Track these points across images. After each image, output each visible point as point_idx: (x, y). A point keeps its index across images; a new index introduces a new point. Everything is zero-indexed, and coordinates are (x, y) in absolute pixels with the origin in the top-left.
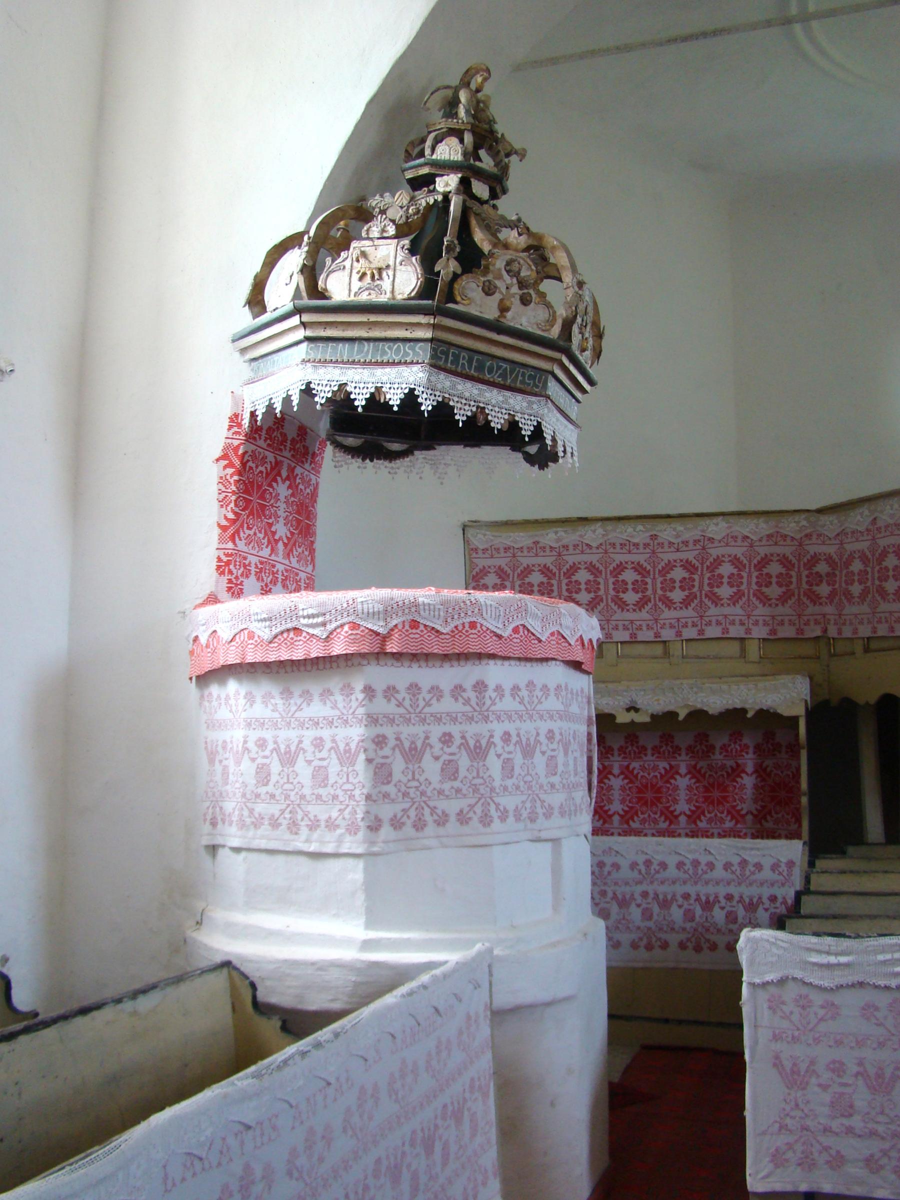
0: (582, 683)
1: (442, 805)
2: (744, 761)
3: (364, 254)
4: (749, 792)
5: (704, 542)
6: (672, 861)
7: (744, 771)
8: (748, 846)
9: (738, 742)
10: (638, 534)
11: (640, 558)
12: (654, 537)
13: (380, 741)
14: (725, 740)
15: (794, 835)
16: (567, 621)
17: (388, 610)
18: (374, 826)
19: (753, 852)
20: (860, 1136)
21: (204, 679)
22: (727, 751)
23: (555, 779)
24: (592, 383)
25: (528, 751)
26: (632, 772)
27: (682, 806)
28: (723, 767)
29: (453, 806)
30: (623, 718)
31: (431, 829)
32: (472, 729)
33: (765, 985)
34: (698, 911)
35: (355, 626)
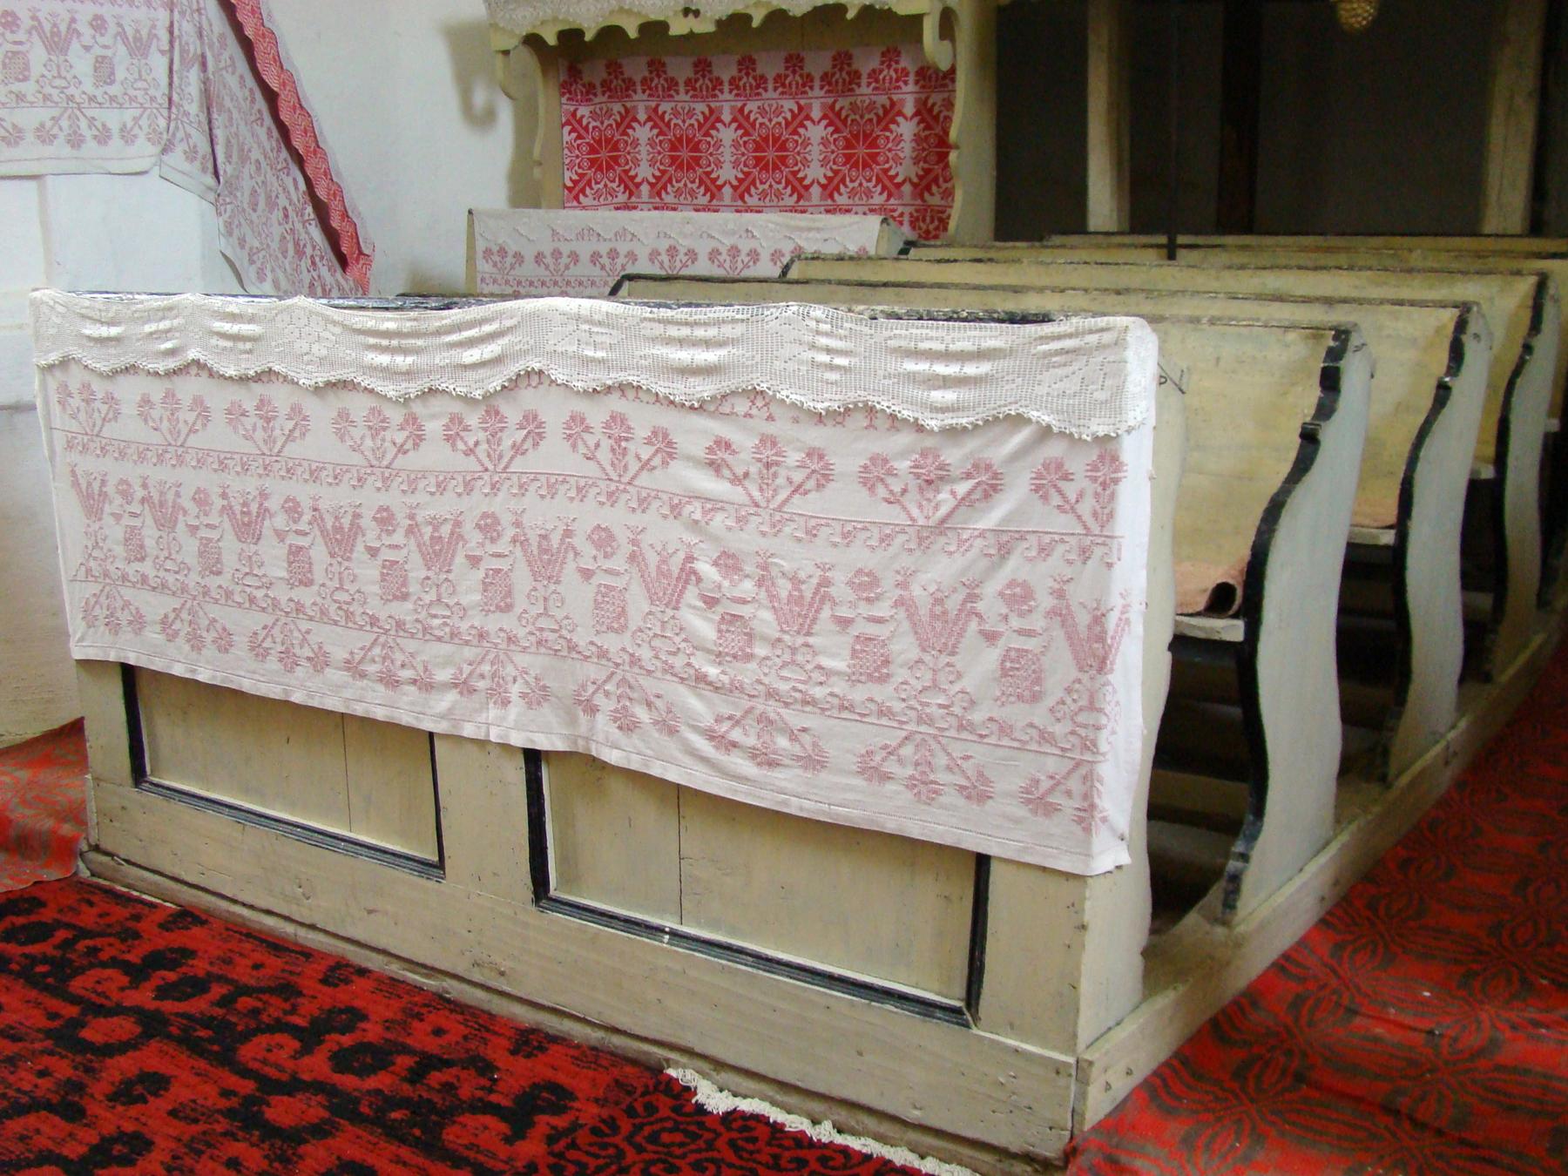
2: (901, 96)
4: (907, 149)
6: (703, 249)
7: (900, 113)
8: (803, 224)
9: (894, 66)
14: (875, 63)
19: (811, 235)
20: (154, 589)
22: (877, 81)
23: (29, 88)
26: (747, 118)
27: (815, 172)
28: (871, 107)
30: (679, 27)
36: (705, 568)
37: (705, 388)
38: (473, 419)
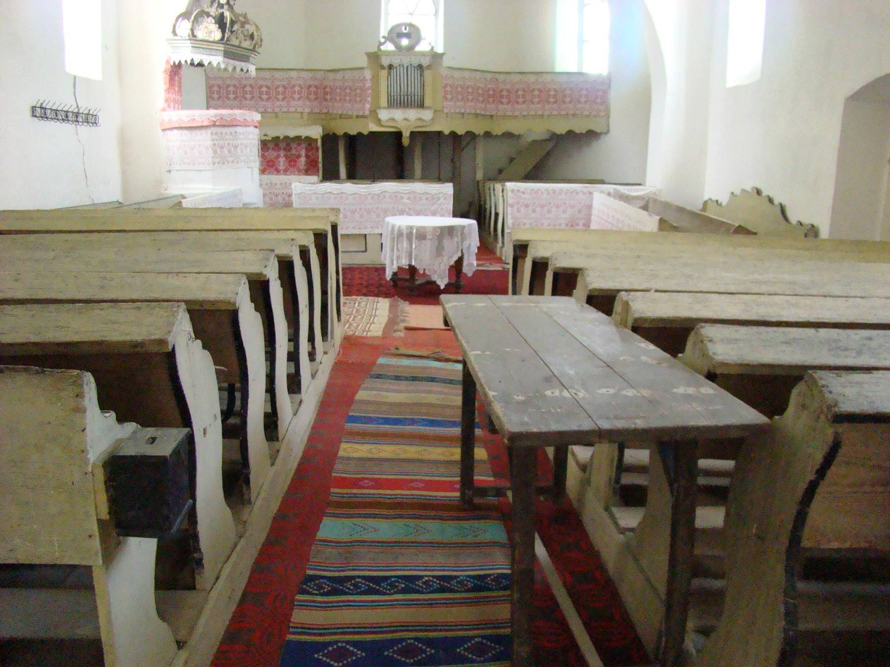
0: (257, 131)
1: (228, 159)
3: (206, 27)
5: (289, 79)
6: (279, 183)
10: (267, 75)
11: (269, 83)
12: (272, 76)
13: (214, 145)
15: (318, 175)
16: (254, 117)
17: (216, 116)
18: (214, 164)
21: (164, 130)
24: (259, 53)
25: (246, 148)
27: (282, 168)
29: (230, 159)
31: (226, 164)
32: (235, 143)
33: (297, 194)
34: (287, 198)
35: (209, 119)
36: (407, 210)
37: (408, 192)
38: (376, 197)
